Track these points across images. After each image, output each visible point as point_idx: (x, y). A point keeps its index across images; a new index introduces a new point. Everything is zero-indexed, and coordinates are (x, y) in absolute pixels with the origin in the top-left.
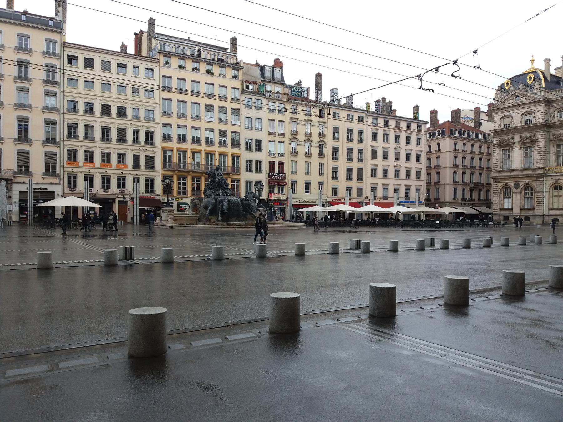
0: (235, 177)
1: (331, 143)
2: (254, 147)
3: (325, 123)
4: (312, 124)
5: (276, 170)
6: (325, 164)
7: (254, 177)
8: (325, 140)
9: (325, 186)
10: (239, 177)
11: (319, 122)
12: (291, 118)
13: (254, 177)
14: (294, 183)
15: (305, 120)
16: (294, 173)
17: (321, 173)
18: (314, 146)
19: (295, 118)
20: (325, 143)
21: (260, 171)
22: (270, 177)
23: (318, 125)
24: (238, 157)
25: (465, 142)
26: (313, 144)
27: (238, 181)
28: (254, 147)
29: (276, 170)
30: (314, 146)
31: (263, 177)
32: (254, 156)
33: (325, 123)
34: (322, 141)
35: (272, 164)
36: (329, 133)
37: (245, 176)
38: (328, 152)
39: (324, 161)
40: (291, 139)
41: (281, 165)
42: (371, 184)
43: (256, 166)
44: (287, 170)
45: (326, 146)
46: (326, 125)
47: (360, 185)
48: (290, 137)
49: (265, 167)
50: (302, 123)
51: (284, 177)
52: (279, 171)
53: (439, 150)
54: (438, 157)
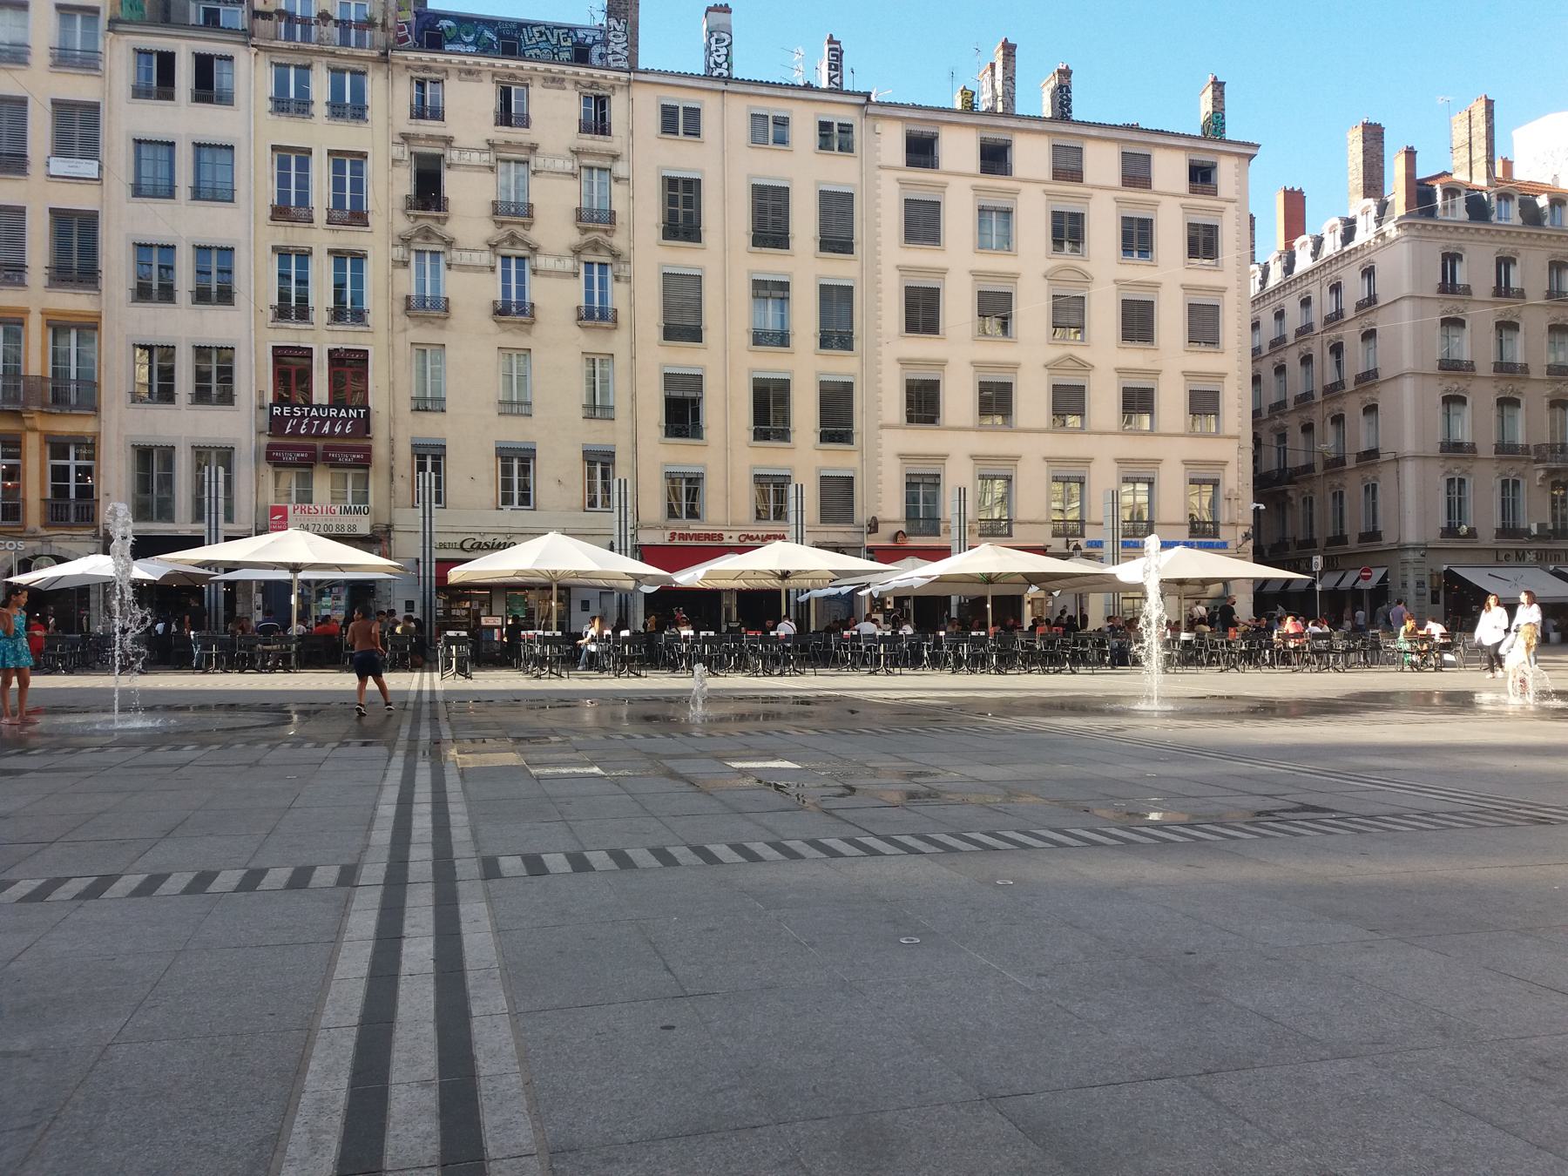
0: (67, 426)
1: (649, 255)
2: (184, 279)
3: (615, 157)
4: (537, 162)
5: (321, 390)
6: (621, 360)
7: (184, 425)
8: (618, 241)
9: (621, 470)
10: (84, 426)
11: (576, 153)
12: (406, 138)
13: (184, 425)
14: (430, 457)
15: (492, 145)
16: (428, 404)
17: (597, 409)
18: (548, 273)
19: (430, 137)
20: (616, 256)
21: (227, 398)
22: (277, 424)
23: (568, 166)
24: (88, 327)
25: (1507, 248)
26: (541, 262)
27: (89, 446)
28: (184, 279)
29: (321, 390)
30: (548, 273)
31: (238, 425)
32: (184, 325)
33: (615, 157)
34: (596, 246)
35: (290, 368)
36: (642, 211)
37: (122, 425)
38: (640, 301)
39: (617, 343)
40: (406, 241)
41: (350, 366)
42: (902, 456)
43: (201, 376)
44: (386, 389)
45: (624, 270)
46: (620, 169)
47: (838, 460)
48: (403, 225)
49: (254, 379)
50: (475, 158)
51: (363, 426)
52: (337, 401)
53: (1371, 300)
54: (1369, 335)
